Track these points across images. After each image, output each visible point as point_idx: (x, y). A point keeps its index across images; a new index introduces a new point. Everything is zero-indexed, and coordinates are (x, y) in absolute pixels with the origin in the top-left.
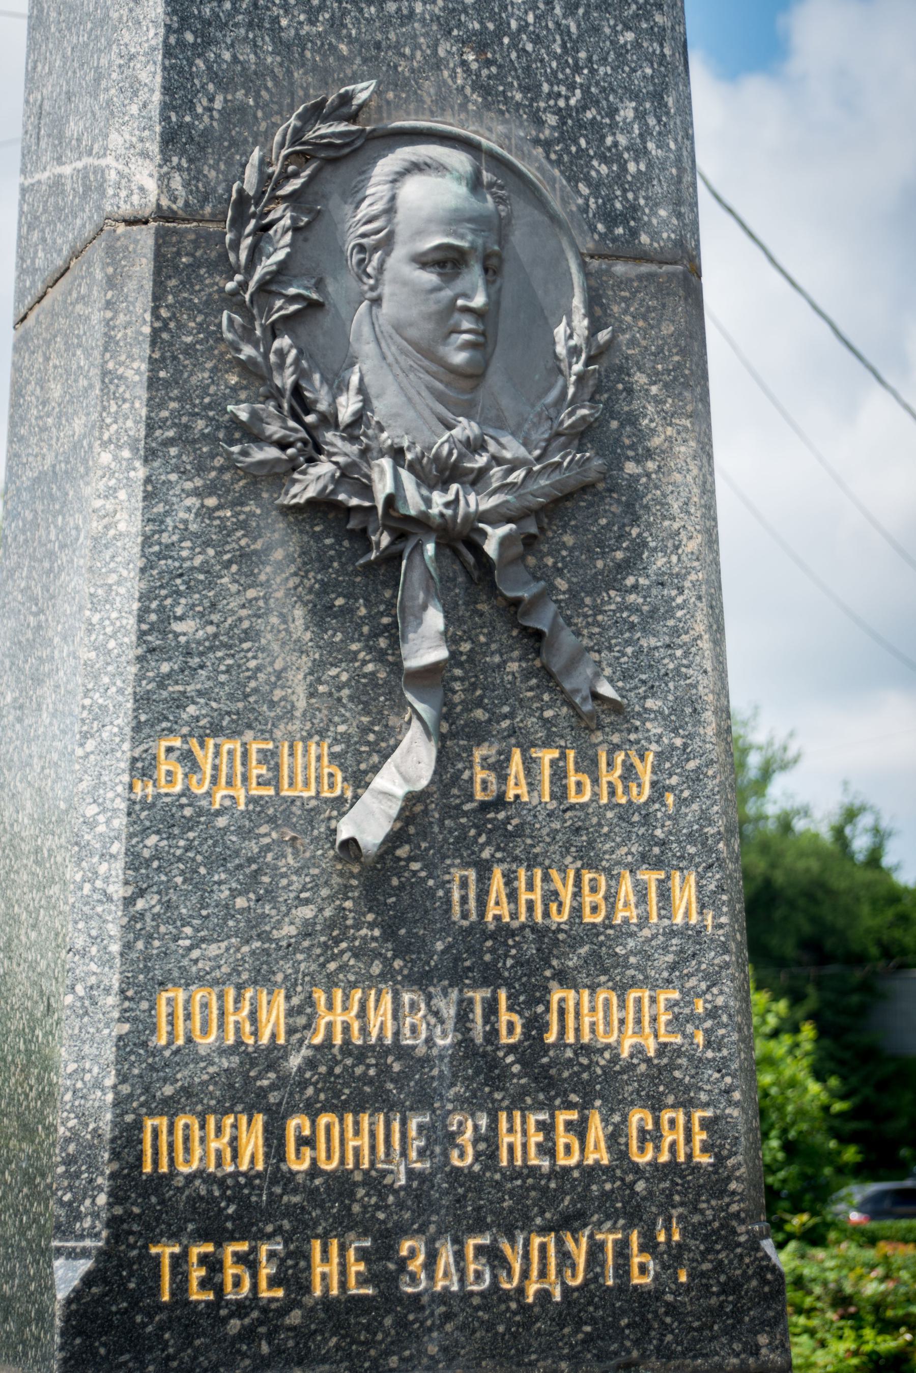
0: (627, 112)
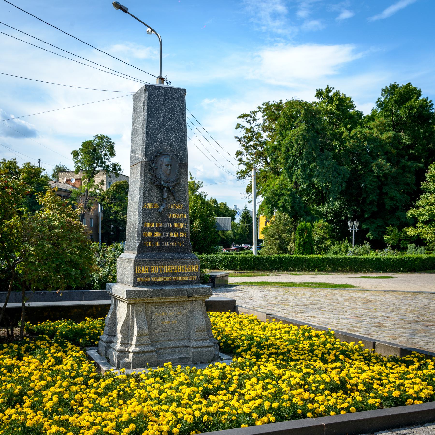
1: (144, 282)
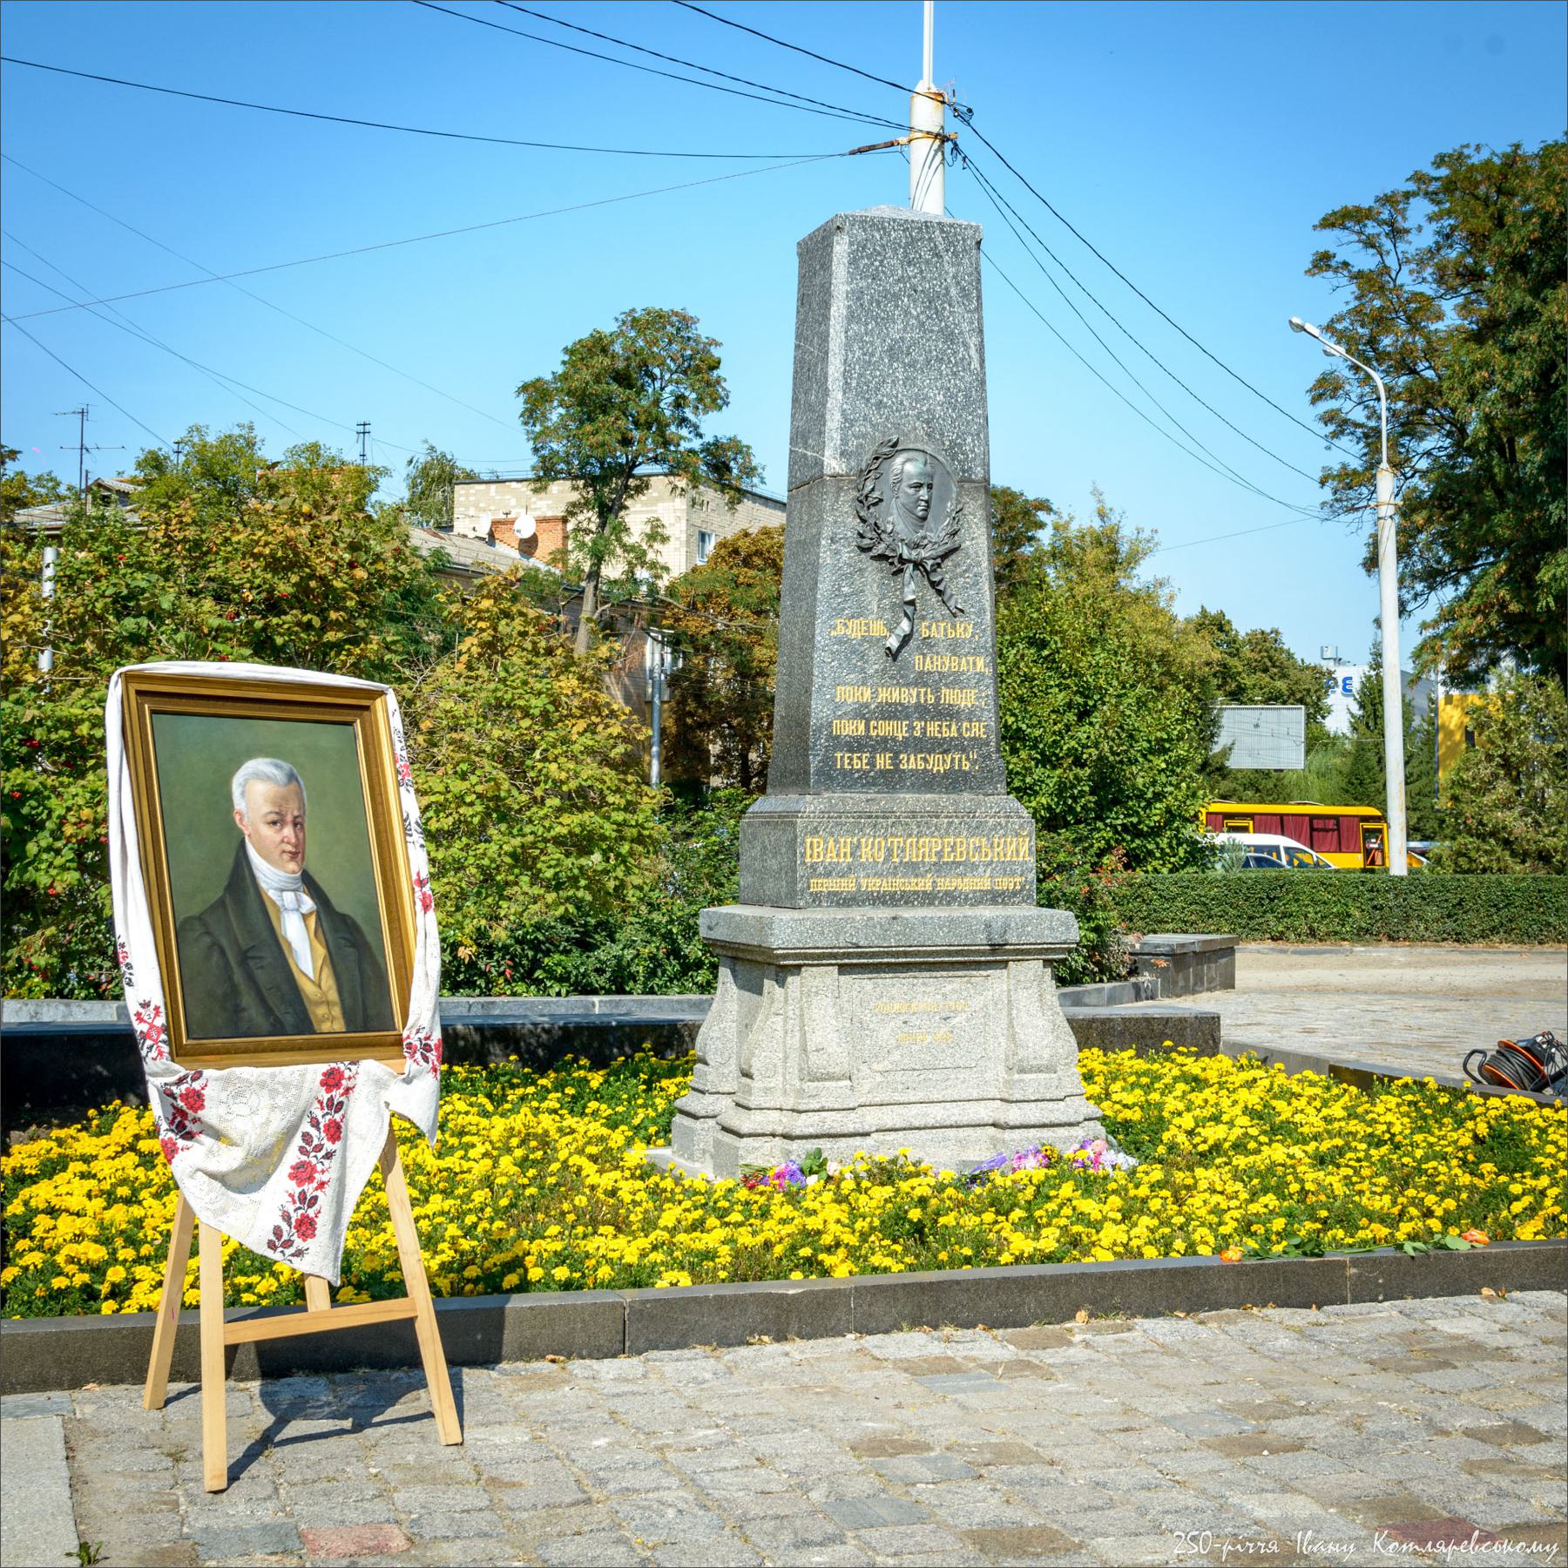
0: (969, 440)
1: (836, 894)
